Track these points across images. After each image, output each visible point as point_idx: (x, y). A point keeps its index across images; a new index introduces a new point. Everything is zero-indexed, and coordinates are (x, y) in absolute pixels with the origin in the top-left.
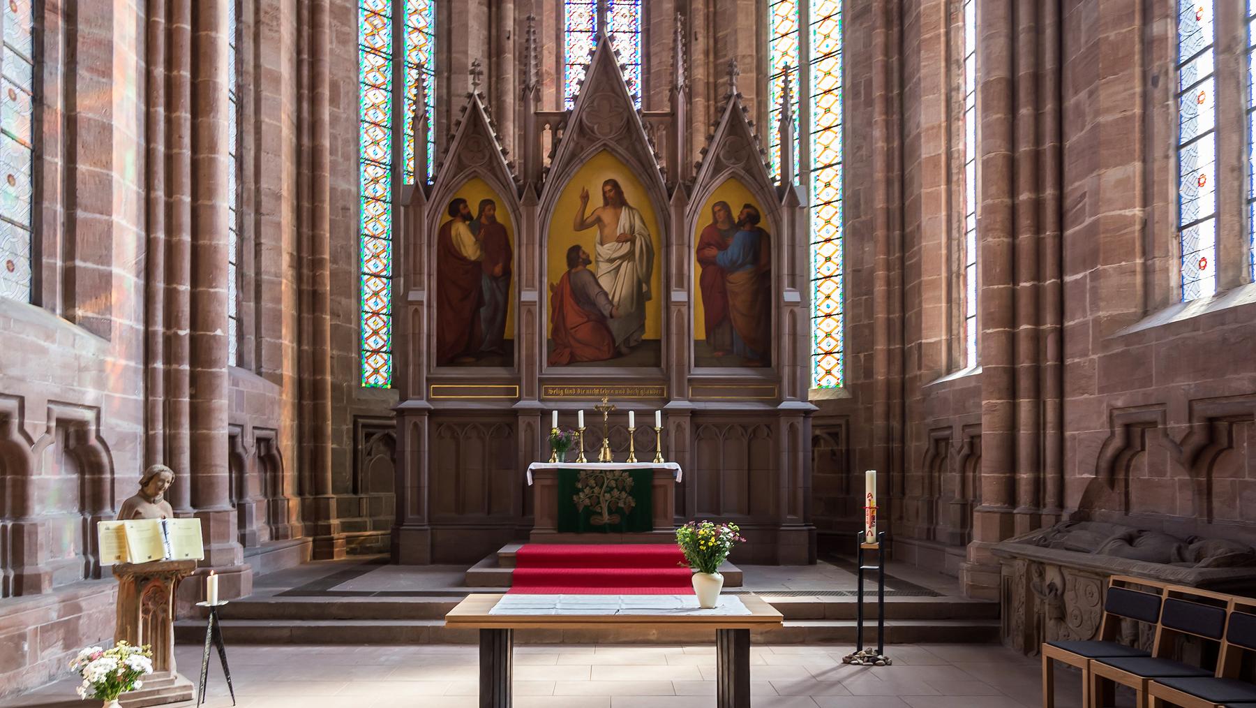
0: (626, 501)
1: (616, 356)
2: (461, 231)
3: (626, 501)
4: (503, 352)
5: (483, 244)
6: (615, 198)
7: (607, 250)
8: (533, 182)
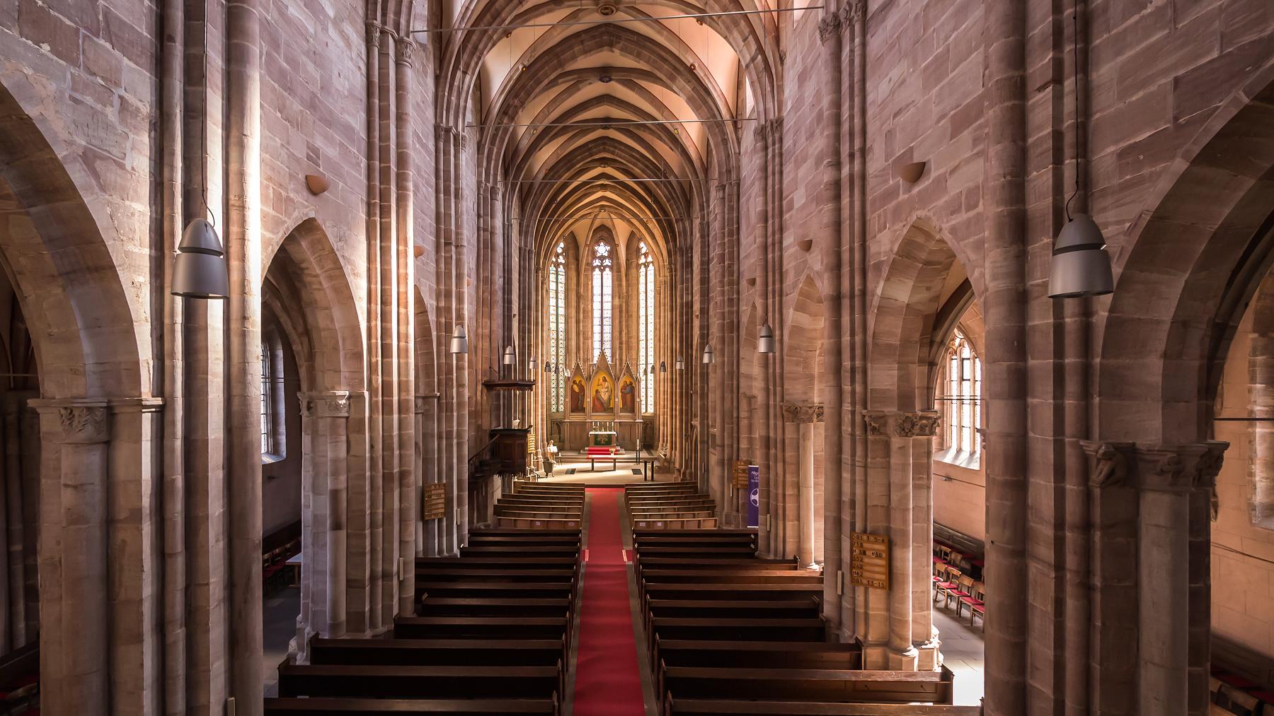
1: (605, 410)
4: (583, 410)
6: (605, 380)
8: (589, 378)
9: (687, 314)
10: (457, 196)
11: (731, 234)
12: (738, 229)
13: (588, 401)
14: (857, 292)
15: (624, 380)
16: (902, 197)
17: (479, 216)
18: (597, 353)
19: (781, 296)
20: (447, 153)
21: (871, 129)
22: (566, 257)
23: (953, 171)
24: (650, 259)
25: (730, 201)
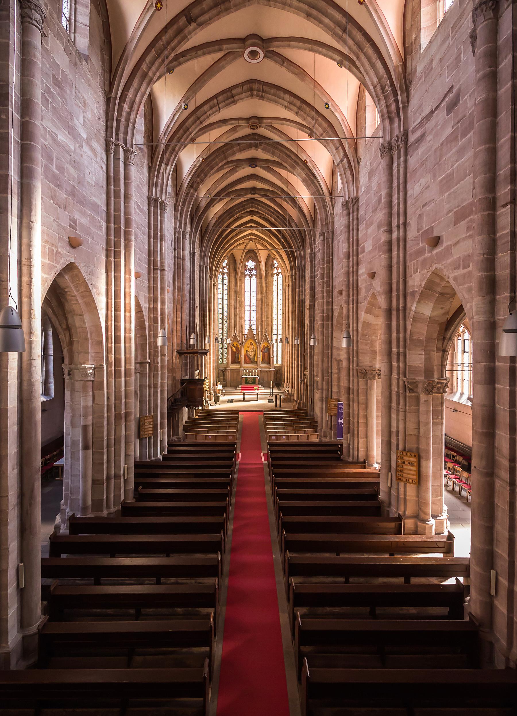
0: (253, 381)
1: (252, 363)
2: (234, 348)
3: (253, 381)
4: (238, 362)
5: (236, 349)
6: (252, 344)
7: (251, 350)
8: (242, 343)
9: (302, 307)
10: (162, 239)
11: (328, 262)
12: (332, 259)
13: (242, 357)
14: (401, 308)
15: (263, 344)
16: (427, 255)
17: (175, 249)
18: (247, 327)
19: (357, 303)
20: (155, 214)
21: (410, 211)
22: (229, 269)
23: (456, 244)
24: (280, 271)
25: (328, 242)
